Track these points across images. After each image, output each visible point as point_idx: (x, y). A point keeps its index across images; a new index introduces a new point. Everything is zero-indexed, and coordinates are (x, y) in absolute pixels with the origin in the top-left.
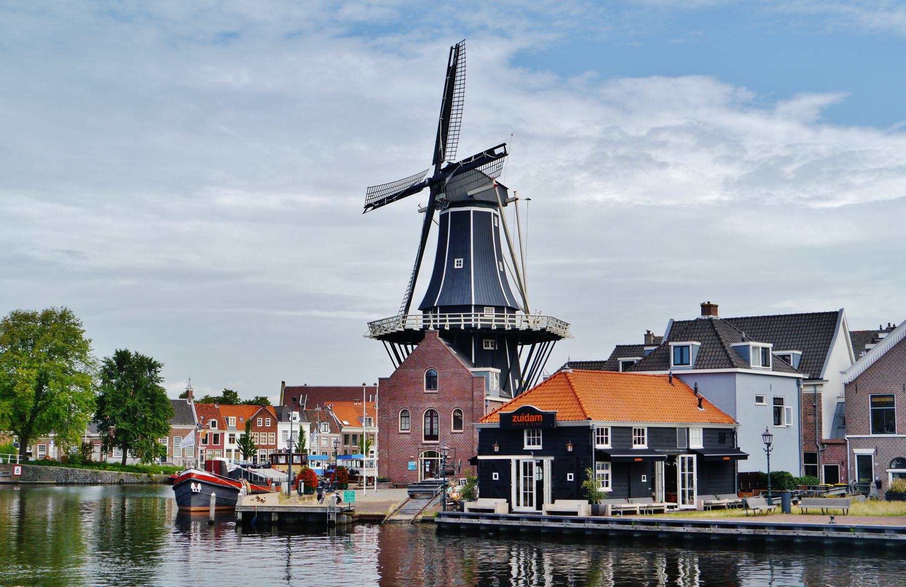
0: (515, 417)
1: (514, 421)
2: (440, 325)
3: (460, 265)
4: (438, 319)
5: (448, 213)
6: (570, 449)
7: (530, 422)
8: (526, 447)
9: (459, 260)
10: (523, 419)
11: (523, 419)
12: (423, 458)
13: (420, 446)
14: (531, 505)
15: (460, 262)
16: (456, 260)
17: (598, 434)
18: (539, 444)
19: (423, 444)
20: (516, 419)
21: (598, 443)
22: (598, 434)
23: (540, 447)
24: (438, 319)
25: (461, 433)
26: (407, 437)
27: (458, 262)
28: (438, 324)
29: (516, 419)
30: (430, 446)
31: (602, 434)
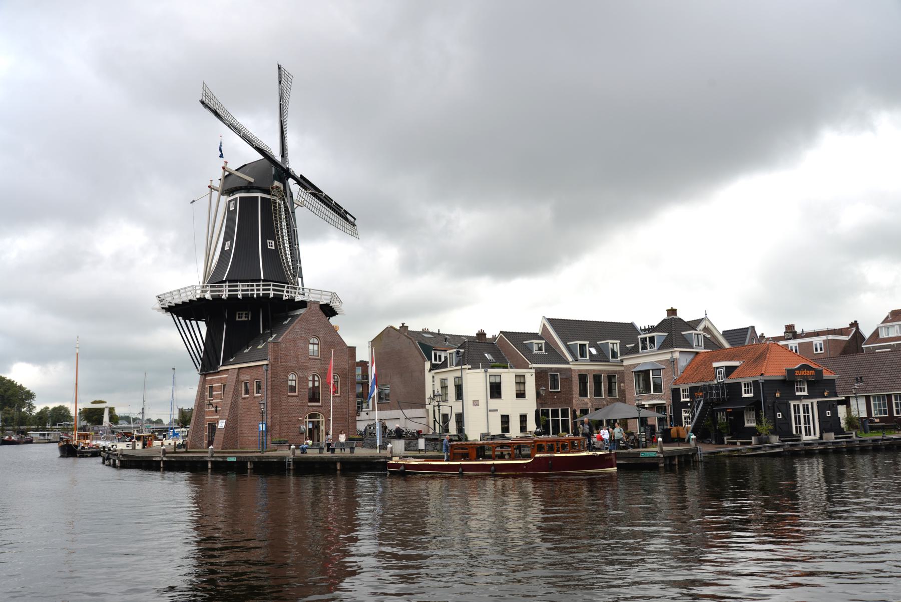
0: (797, 372)
1: (796, 374)
2: (228, 295)
3: (272, 246)
4: (261, 288)
5: (258, 197)
6: (778, 395)
7: (807, 376)
8: (798, 394)
9: (271, 241)
10: (802, 373)
11: (802, 373)
12: (308, 420)
13: (306, 408)
14: (810, 435)
15: (272, 243)
16: (268, 241)
17: (751, 389)
18: (804, 391)
19: (309, 406)
20: (798, 373)
21: (798, 391)
22: (751, 389)
23: (806, 393)
24: (261, 288)
25: (338, 397)
26: (295, 399)
27: (269, 243)
28: (261, 292)
29: (798, 373)
30: (314, 408)
31: (748, 387)
